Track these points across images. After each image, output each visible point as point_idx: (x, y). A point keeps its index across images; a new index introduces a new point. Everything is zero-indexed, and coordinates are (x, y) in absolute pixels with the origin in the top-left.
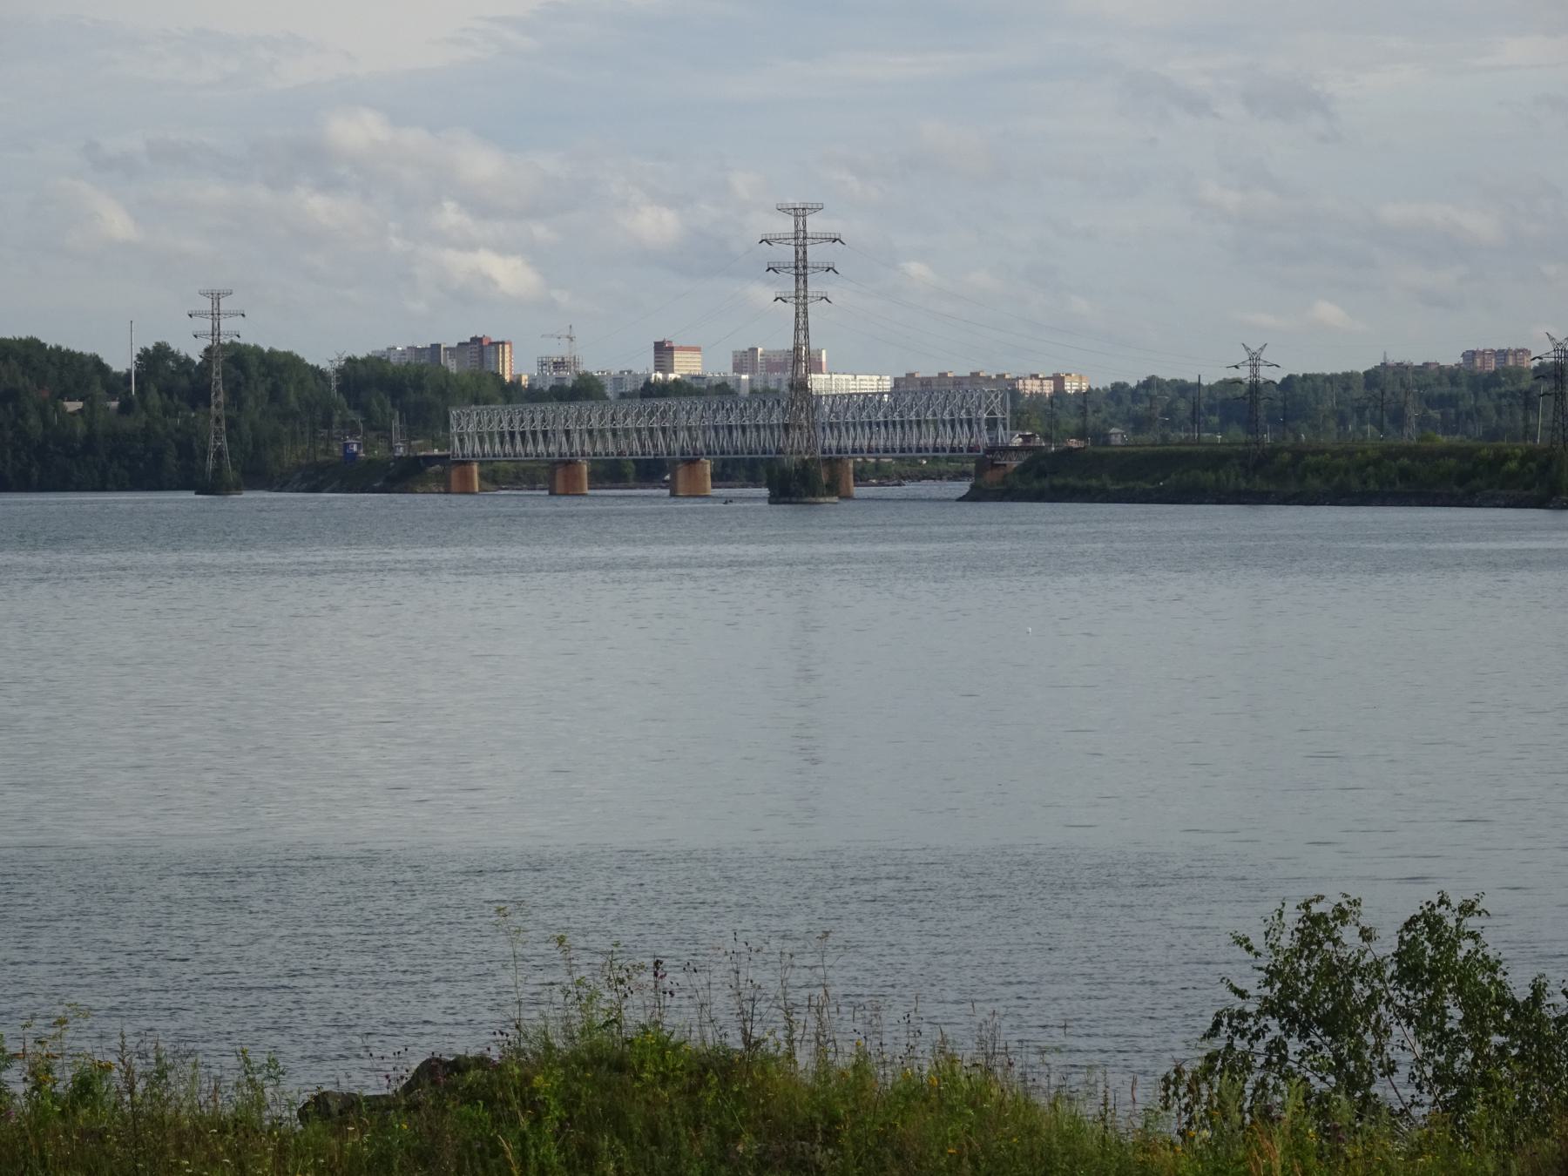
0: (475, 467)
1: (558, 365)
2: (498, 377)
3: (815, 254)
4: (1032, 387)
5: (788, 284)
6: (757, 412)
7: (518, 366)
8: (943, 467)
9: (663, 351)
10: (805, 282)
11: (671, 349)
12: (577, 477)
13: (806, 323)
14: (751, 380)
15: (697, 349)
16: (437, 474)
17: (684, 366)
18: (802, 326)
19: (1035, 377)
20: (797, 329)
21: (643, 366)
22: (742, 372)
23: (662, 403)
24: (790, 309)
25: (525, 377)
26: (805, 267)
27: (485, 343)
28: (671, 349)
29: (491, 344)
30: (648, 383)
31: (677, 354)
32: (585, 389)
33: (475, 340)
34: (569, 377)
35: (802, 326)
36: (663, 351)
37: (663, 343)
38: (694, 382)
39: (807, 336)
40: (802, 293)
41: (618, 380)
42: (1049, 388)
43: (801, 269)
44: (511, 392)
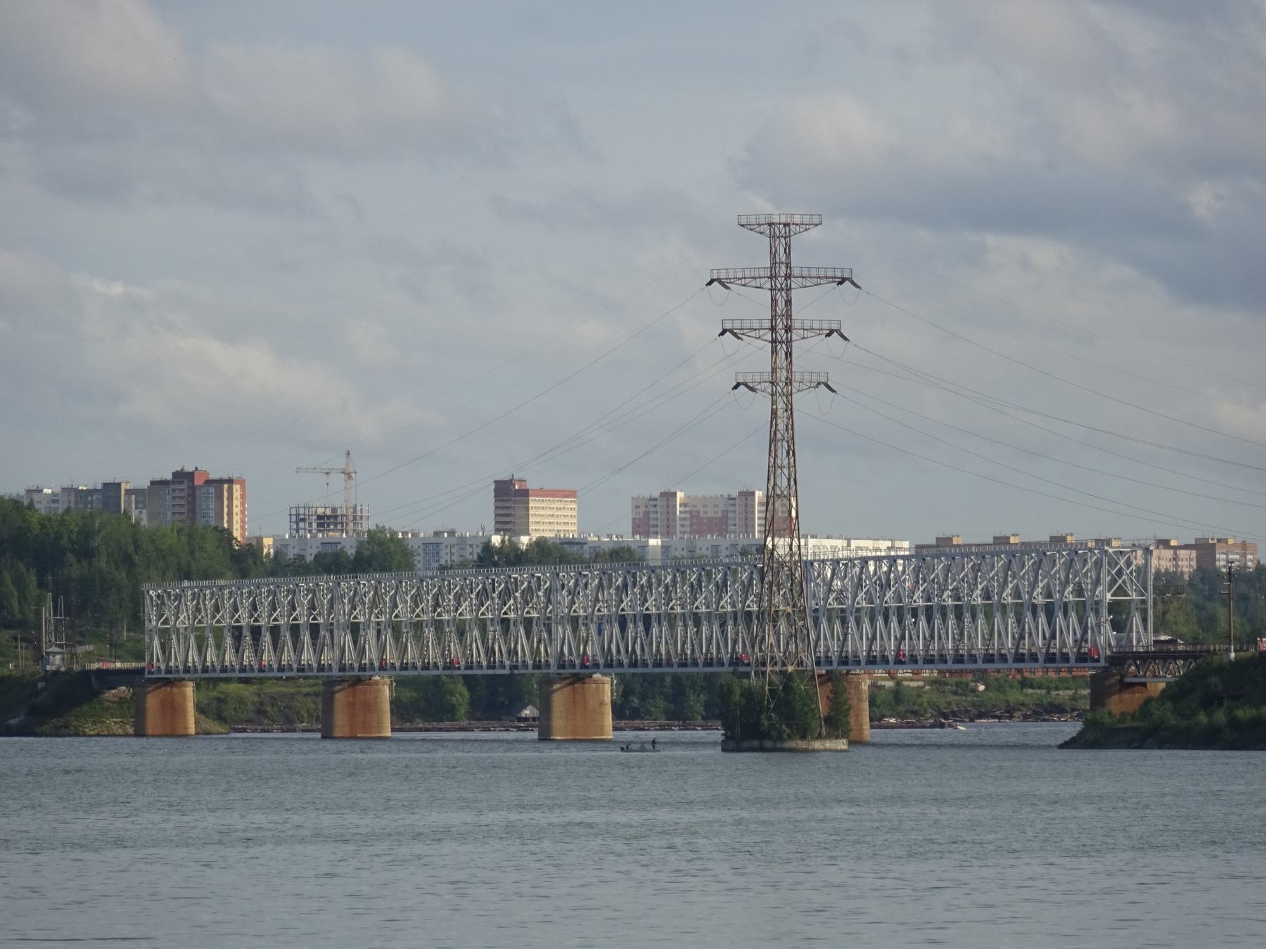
0: (189, 689)
1: (325, 521)
2: (225, 536)
3: (809, 305)
4: (1161, 561)
5: (755, 355)
6: (695, 589)
7: (256, 519)
8: (1014, 696)
9: (510, 498)
10: (789, 354)
11: (525, 493)
12: (371, 707)
13: (790, 427)
14: (665, 548)
15: (570, 494)
16: (121, 701)
17: (549, 520)
18: (781, 439)
19: (1165, 544)
20: (773, 440)
21: (477, 522)
22: (648, 534)
23: (522, 576)
24: (760, 405)
25: (268, 542)
26: (788, 329)
27: (198, 481)
28: (525, 493)
29: (209, 482)
30: (487, 546)
31: (533, 503)
32: (381, 555)
33: (180, 476)
34: (346, 540)
35: (781, 439)
36: (510, 498)
37: (510, 483)
38: (568, 548)
39: (791, 452)
40: (782, 375)
41: (432, 547)
42: (1187, 563)
43: (781, 333)
44: (245, 561)
